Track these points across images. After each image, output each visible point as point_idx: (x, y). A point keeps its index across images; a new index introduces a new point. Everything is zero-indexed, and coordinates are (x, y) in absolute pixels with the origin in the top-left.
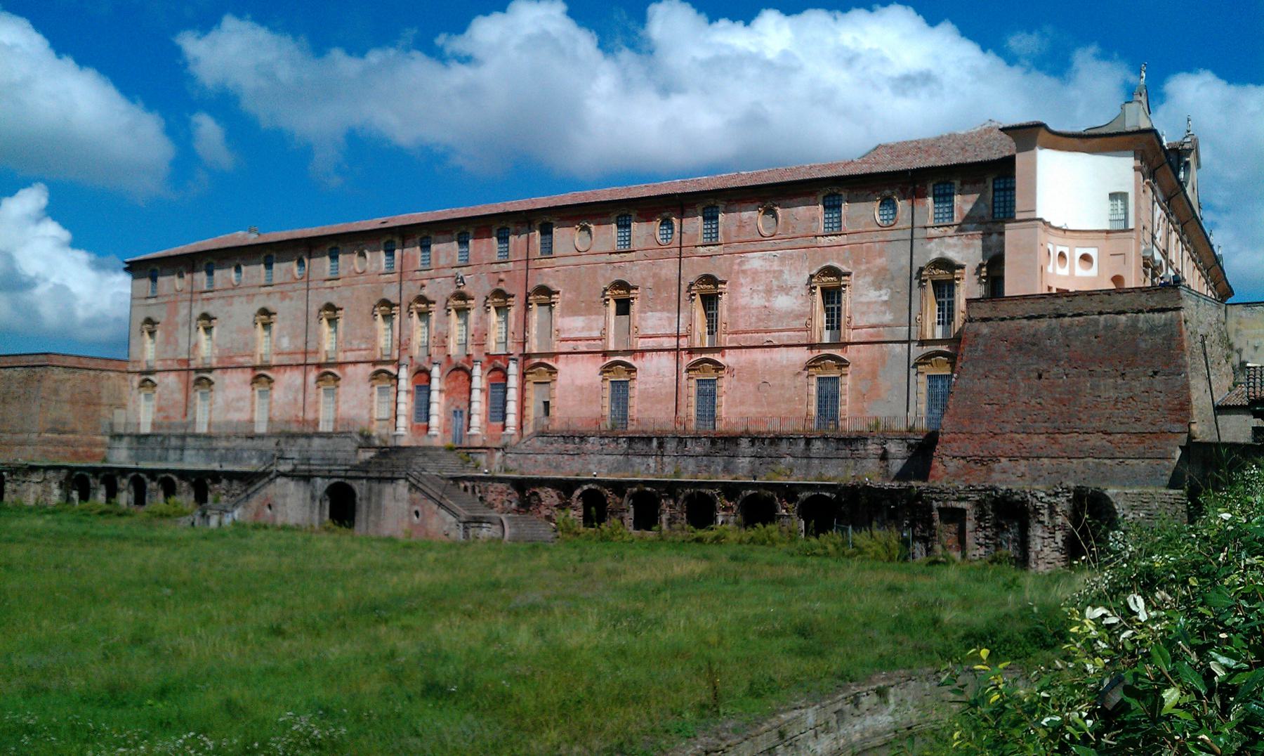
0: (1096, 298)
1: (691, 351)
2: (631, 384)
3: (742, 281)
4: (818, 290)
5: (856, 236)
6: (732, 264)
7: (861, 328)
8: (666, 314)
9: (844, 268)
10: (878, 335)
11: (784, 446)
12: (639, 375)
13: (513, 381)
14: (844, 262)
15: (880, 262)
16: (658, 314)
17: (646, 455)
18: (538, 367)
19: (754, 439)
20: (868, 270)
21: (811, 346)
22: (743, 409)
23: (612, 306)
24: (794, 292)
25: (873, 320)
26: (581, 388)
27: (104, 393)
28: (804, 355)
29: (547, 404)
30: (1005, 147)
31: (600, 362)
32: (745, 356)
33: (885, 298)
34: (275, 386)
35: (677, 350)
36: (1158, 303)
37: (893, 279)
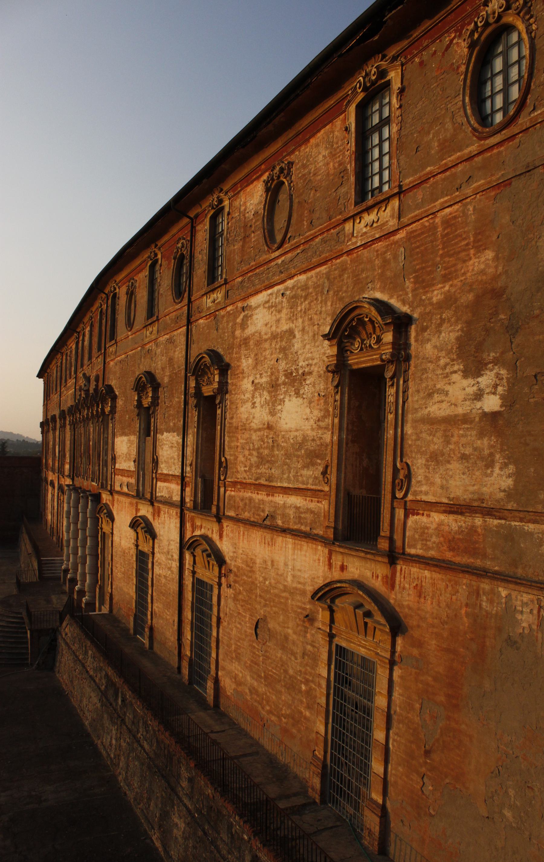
10: (466, 542)
14: (394, 286)
15: (481, 263)
20: (449, 301)
24: (307, 390)
25: (459, 483)
33: (492, 403)
37: (512, 329)
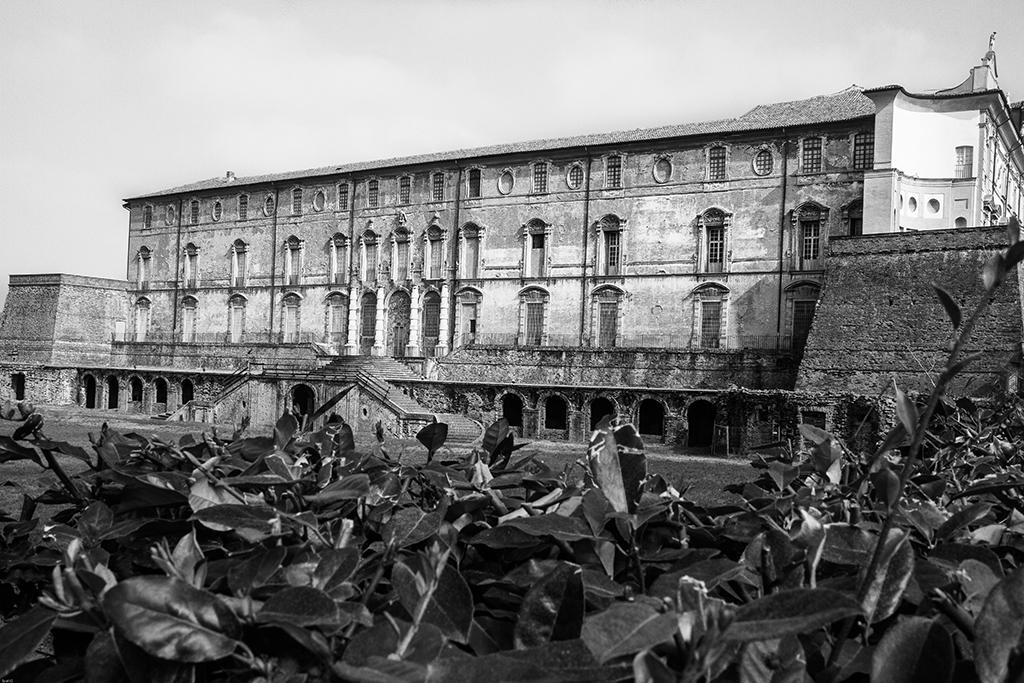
0: (942, 237)
1: (595, 279)
2: (545, 306)
3: (640, 220)
4: (704, 229)
5: (736, 183)
6: (631, 207)
7: (740, 260)
8: (575, 247)
9: (727, 210)
11: (673, 361)
12: (551, 299)
13: (445, 304)
14: (727, 205)
16: (569, 247)
17: (555, 366)
18: (468, 292)
19: (648, 353)
20: (747, 211)
21: (697, 276)
22: (639, 328)
23: (529, 240)
27: (108, 309)
28: (690, 284)
29: (473, 323)
30: (866, 107)
31: (520, 288)
33: (762, 236)
34: (248, 304)
35: (583, 279)
36: (996, 240)
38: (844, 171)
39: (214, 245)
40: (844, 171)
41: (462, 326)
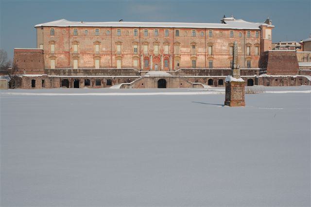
26: (186, 61)
32: (217, 57)
38: (254, 38)
39: (87, 43)
40: (254, 38)
41: (176, 65)
